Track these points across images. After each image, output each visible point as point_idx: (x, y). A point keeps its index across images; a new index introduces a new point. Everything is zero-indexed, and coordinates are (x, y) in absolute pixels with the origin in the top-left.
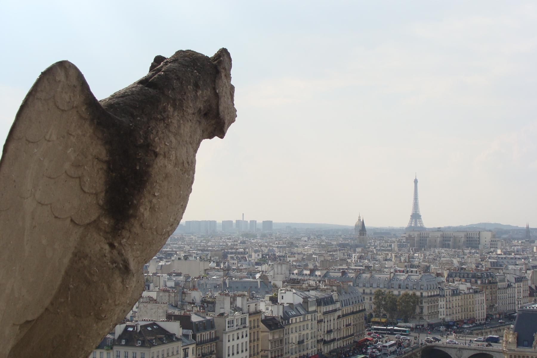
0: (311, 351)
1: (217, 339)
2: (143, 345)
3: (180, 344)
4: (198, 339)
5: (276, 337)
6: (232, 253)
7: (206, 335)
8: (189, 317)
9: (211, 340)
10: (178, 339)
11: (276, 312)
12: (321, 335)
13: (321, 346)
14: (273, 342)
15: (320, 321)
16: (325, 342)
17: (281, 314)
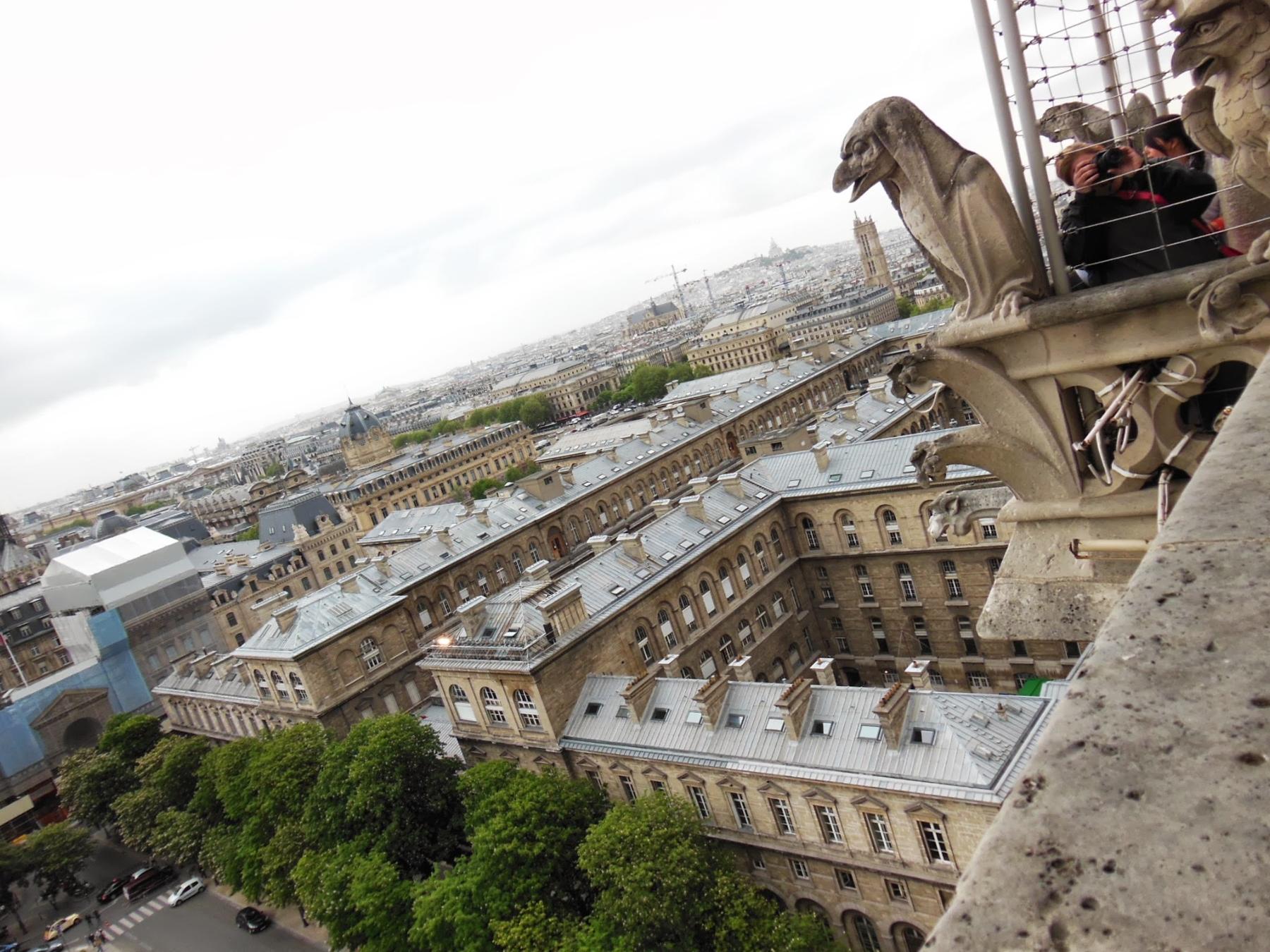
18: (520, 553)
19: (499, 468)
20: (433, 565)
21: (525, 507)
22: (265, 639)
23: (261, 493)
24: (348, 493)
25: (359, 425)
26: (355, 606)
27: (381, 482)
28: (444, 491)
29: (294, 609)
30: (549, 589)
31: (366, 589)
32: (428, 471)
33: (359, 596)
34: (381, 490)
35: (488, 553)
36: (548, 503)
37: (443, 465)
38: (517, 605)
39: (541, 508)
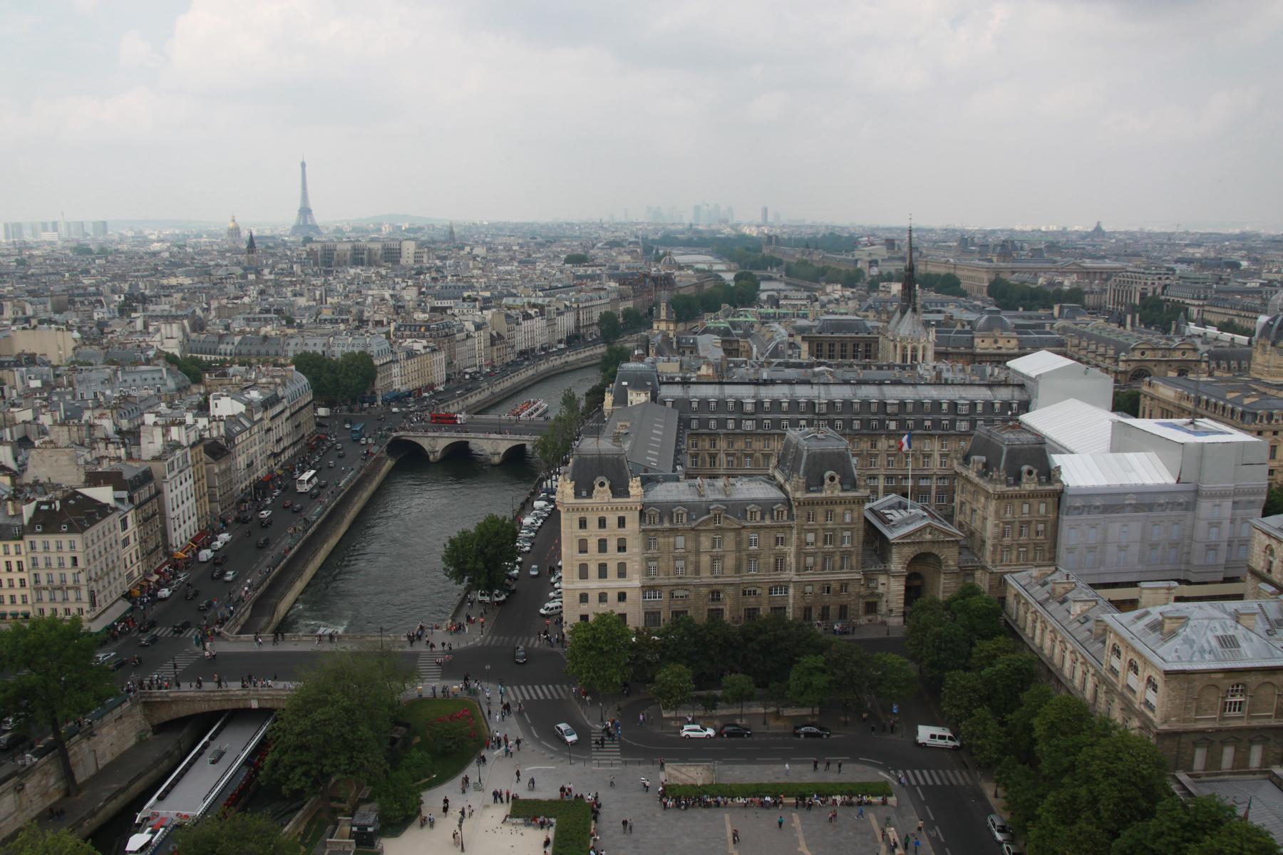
0: (261, 473)
1: (159, 492)
2: (69, 532)
3: (116, 515)
4: (137, 502)
5: (223, 467)
6: (79, 295)
7: (145, 493)
8: (120, 474)
9: (151, 498)
10: (115, 509)
11: (218, 432)
12: (271, 448)
13: (272, 462)
14: (223, 473)
15: (269, 430)
16: (275, 455)
17: (222, 431)
23: (1143, 354)
24: (1243, 415)
26: (1244, 644)
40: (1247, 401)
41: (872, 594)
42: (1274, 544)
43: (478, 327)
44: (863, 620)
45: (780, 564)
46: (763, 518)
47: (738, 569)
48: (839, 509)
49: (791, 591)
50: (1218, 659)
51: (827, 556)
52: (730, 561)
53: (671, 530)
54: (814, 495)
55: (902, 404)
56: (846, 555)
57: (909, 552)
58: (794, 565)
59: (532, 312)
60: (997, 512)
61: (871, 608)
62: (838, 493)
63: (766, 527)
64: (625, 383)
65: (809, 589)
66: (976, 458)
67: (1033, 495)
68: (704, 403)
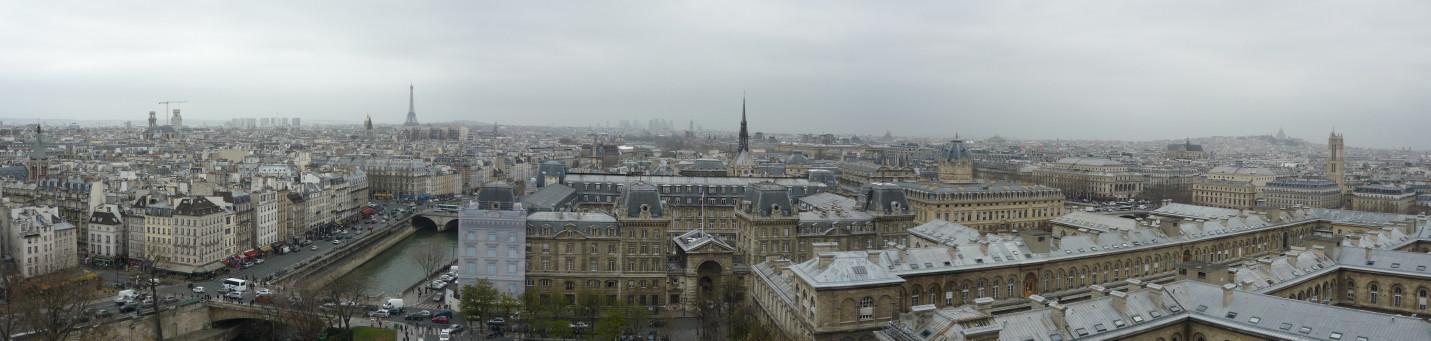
18: (1000, 282)
19: (1034, 215)
20: (935, 265)
21: (1018, 251)
22: (810, 267)
24: (929, 195)
25: (954, 152)
26: (869, 271)
27: (953, 196)
28: (991, 218)
29: (832, 257)
30: (982, 321)
31: (885, 264)
32: (985, 200)
33: (876, 266)
34: (949, 200)
35: (977, 274)
36: (1034, 255)
37: (997, 199)
38: (953, 323)
39: (1028, 256)
40: (931, 189)
41: (675, 290)
42: (920, 240)
43: (486, 164)
44: (670, 308)
45: (612, 265)
46: (600, 234)
47: (584, 267)
48: (650, 230)
49: (619, 285)
50: (852, 281)
51: (644, 261)
52: (578, 262)
53: (540, 239)
54: (633, 219)
55: (719, 188)
56: (656, 260)
57: (699, 260)
58: (621, 267)
59: (523, 159)
60: (756, 235)
61: (675, 299)
62: (649, 218)
63: (602, 240)
64: (544, 173)
65: (631, 283)
66: (745, 202)
67: (779, 223)
68: (592, 185)
